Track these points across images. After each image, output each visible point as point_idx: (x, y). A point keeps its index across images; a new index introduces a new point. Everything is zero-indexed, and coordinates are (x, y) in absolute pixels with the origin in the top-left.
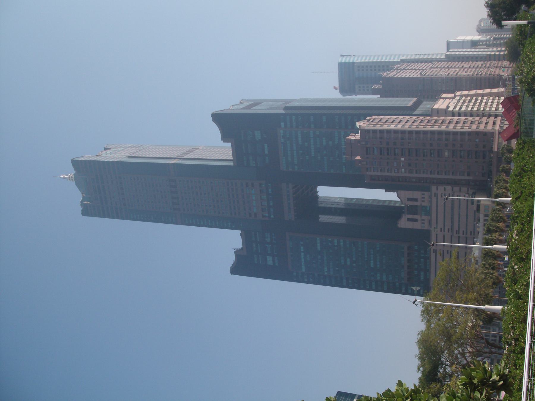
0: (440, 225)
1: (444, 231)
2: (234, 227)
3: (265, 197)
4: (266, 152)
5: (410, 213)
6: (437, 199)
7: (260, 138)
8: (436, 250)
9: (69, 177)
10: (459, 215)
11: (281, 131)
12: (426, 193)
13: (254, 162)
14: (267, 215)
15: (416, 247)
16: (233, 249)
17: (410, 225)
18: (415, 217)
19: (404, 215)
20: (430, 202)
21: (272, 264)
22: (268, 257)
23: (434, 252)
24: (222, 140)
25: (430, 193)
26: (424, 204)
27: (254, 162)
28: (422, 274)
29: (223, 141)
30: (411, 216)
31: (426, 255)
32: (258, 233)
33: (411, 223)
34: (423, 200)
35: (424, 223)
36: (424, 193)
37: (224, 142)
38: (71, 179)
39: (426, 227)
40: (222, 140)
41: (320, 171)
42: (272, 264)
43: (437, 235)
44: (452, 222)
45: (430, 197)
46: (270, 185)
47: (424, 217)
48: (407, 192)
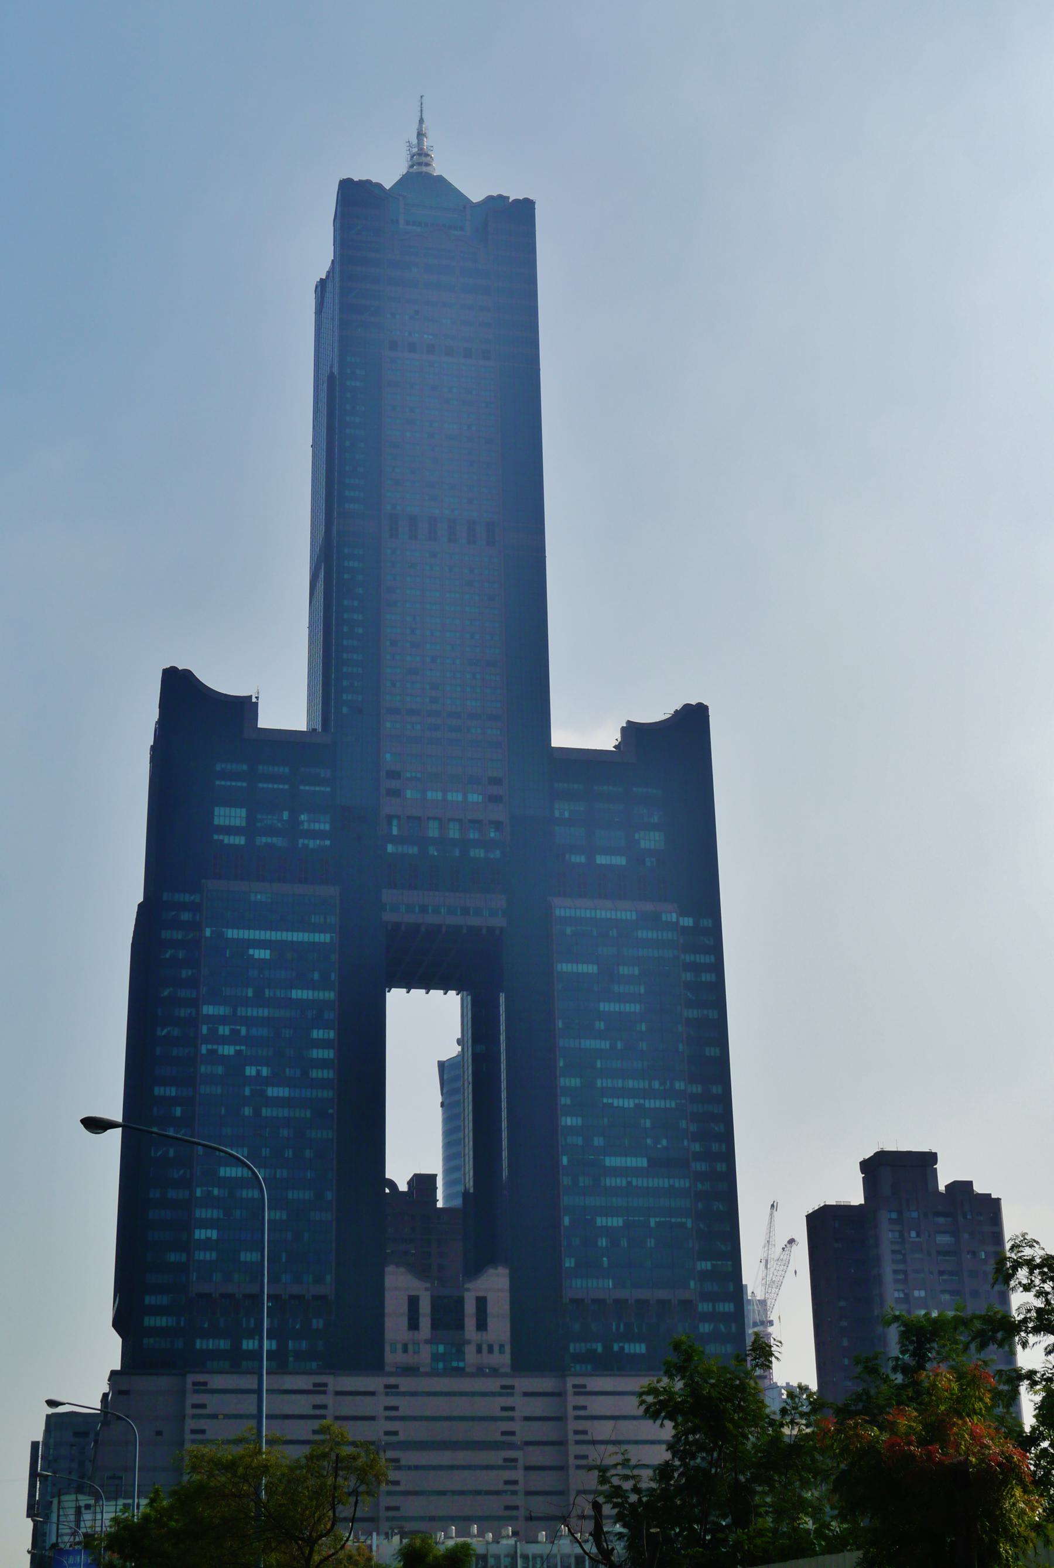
0: (406, 1406)
1: (388, 1418)
2: (345, 710)
3: (454, 832)
4: (601, 860)
5: (436, 1305)
6: (493, 1394)
8: (324, 1392)
10: (452, 1467)
11: (674, 917)
12: (506, 1358)
14: (395, 831)
15: (317, 1324)
16: (258, 693)
17: (395, 1306)
18: (425, 1323)
19: (428, 1285)
20: (480, 1372)
21: (216, 822)
22: (243, 812)
23: (315, 1385)
24: (629, 722)
25: (508, 1370)
26: (470, 1351)
27: (567, 815)
28: (223, 1344)
29: (625, 725)
30: (425, 1307)
31: (291, 1359)
32: (328, 789)
33: (404, 1308)
34: (485, 1348)
35: (405, 1350)
36: (508, 1349)
39: (392, 1357)
41: (560, 1024)
42: (216, 822)
43: (372, 1394)
44: (421, 1445)
45: (495, 1372)
46: (498, 854)
47: (426, 1351)
48: (506, 1296)
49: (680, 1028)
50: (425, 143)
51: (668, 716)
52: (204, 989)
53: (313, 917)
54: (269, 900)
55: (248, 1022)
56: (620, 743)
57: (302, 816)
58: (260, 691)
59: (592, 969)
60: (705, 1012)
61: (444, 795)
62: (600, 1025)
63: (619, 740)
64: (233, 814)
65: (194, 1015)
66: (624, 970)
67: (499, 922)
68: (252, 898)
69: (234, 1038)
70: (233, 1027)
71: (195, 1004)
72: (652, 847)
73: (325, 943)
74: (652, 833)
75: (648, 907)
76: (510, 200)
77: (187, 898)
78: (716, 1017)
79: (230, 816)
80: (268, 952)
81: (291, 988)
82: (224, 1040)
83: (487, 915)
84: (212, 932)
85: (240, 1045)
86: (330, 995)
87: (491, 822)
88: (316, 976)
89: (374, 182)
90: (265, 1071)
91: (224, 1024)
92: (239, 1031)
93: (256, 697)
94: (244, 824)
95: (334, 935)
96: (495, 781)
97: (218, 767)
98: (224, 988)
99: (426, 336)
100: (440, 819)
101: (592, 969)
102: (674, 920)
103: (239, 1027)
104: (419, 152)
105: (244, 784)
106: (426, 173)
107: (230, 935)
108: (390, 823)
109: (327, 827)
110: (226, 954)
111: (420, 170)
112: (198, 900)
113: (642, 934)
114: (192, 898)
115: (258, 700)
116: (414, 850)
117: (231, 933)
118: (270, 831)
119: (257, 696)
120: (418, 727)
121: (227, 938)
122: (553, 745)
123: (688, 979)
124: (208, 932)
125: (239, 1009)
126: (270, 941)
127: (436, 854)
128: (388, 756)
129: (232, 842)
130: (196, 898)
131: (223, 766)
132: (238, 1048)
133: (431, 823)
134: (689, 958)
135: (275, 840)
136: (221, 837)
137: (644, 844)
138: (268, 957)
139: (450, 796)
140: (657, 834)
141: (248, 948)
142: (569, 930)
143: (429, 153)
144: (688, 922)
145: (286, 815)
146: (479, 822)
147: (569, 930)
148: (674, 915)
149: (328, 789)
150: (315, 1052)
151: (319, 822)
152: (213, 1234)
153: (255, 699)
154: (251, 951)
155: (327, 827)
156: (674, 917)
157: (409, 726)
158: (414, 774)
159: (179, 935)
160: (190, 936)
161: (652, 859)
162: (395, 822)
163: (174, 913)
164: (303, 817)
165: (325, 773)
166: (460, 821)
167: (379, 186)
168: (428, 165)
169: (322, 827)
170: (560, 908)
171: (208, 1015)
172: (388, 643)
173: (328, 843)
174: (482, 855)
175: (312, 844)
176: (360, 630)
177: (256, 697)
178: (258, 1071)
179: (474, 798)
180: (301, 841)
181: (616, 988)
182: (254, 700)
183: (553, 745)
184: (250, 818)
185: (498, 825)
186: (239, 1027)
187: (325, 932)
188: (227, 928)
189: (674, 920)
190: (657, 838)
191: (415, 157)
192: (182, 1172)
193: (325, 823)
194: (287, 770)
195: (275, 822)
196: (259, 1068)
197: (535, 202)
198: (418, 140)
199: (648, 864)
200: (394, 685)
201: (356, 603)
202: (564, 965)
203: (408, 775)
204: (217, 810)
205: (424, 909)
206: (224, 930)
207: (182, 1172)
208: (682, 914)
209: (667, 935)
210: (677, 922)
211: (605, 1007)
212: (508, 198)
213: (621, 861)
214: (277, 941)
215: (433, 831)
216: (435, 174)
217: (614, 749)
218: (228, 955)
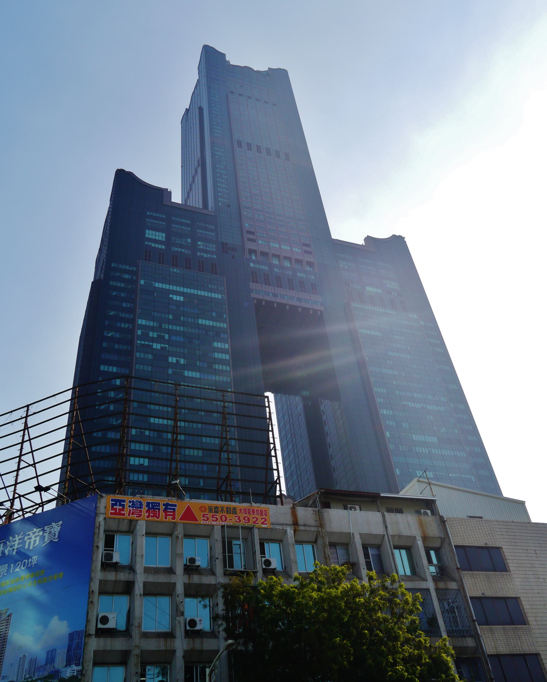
21: (147, 236)
42: (147, 236)
55: (168, 331)
65: (131, 327)
69: (160, 339)
70: (160, 334)
82: (153, 340)
85: (164, 344)
90: (182, 361)
91: (153, 331)
92: (164, 336)
124: (142, 282)
126: (183, 292)
128: (247, 225)
132: (163, 345)
135: (183, 250)
136: (150, 244)
150: (216, 354)
152: (146, 462)
154: (171, 296)
160: (129, 287)
163: (119, 274)
173: (215, 256)
178: (177, 361)
184: (167, 237)
188: (155, 282)
192: (119, 422)
195: (183, 242)
196: (178, 359)
203: (259, 235)
206: (152, 282)
207: (119, 422)
218: (155, 296)
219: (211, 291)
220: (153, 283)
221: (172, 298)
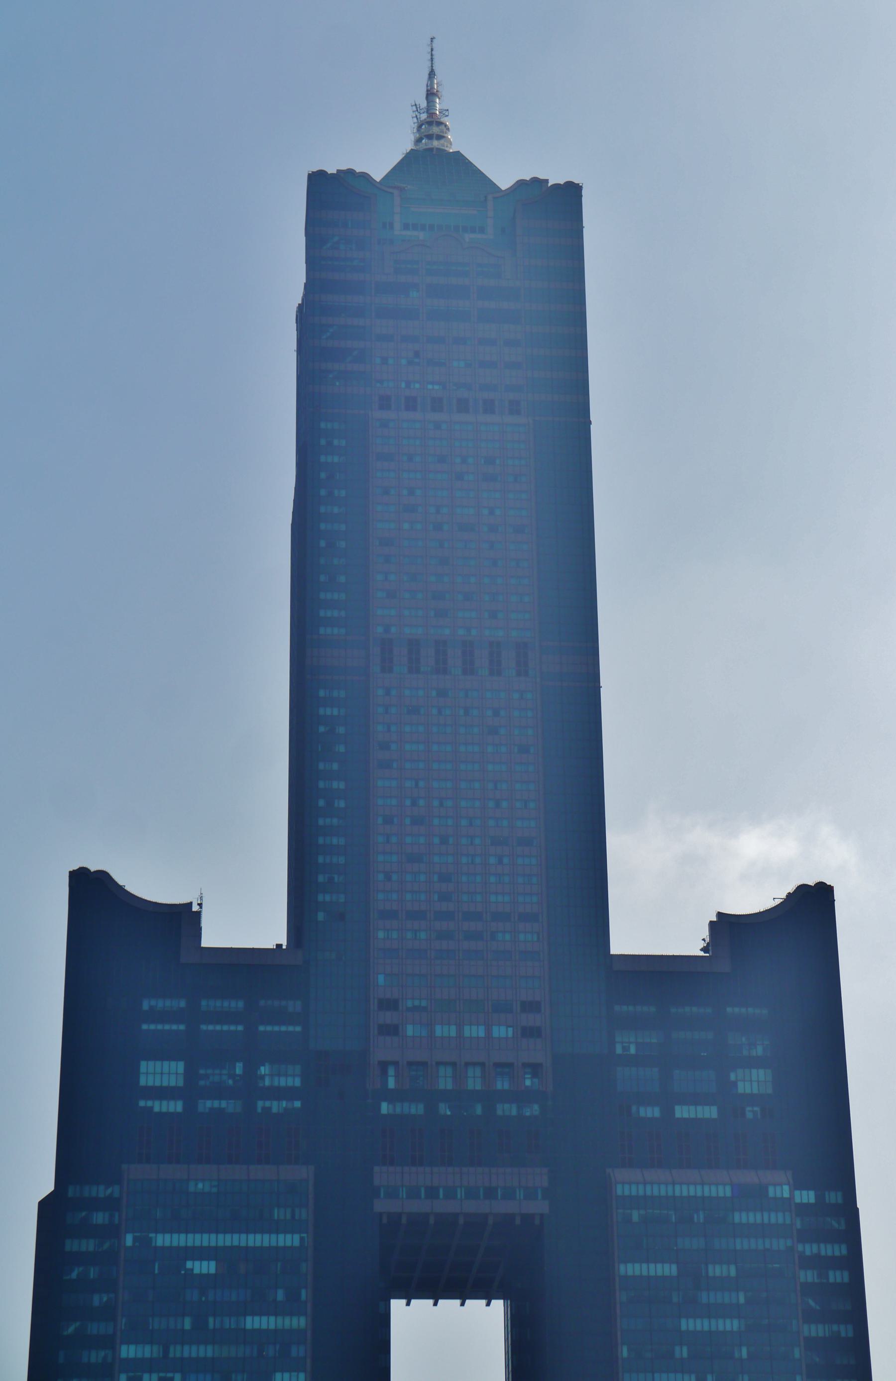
3: (474, 1082)
4: (682, 1112)
7: (742, 1088)
9: (440, 123)
11: (786, 1192)
13: (633, 1050)
14: (391, 1083)
16: (201, 899)
21: (143, 1082)
22: (180, 1066)
24: (720, 915)
27: (633, 1050)
29: (715, 919)
32: (298, 1029)
37: (711, 923)
38: (435, 130)
40: (720, 915)
41: (625, 1352)
42: (143, 1082)
49: (797, 1354)
50: (438, 106)
51: (778, 902)
52: (124, 1321)
53: (276, 1211)
54: (214, 1190)
56: (708, 944)
57: (262, 1068)
58: (203, 895)
59: (669, 1270)
60: (835, 1328)
61: (460, 1030)
62: (683, 1352)
63: (708, 940)
64: (166, 1070)
66: (716, 1270)
67: (539, 1207)
68: (192, 1188)
71: (109, 1343)
72: (755, 1091)
73: (292, 1248)
74: (754, 1071)
75: (748, 1177)
76: (549, 185)
77: (101, 1191)
78: (851, 1334)
79: (162, 1074)
80: (213, 1264)
81: (245, 1315)
83: (522, 1197)
84: (135, 1239)
86: (299, 1322)
87: (525, 1065)
88: (280, 1295)
89: (357, 171)
93: (198, 904)
94: (181, 1083)
95: (305, 1235)
96: (530, 1007)
97: (146, 1006)
98: (150, 1319)
99: (430, 387)
100: (454, 1065)
101: (669, 1270)
102: (786, 1194)
103: (170, 1375)
104: (429, 120)
105: (182, 1027)
106: (438, 149)
107: (159, 1243)
108: (384, 1073)
109: (298, 1082)
110: (154, 1270)
111: (430, 146)
112: (116, 1195)
113: (741, 1218)
114: (109, 1191)
115: (201, 907)
116: (417, 1109)
117: (162, 1240)
118: (219, 1092)
119: (199, 902)
120: (423, 935)
121: (156, 1247)
122: (612, 953)
123: (810, 1280)
124: (129, 1240)
125: (172, 1349)
126: (216, 1248)
127: (449, 1113)
128: (381, 979)
129: (164, 1110)
130: (114, 1191)
131: (153, 1003)
133: (442, 1070)
134: (810, 1249)
135: (224, 1104)
136: (149, 1103)
137: (743, 1088)
138: (213, 1270)
139: (467, 1031)
140: (761, 1072)
141: (186, 1260)
142: (635, 1216)
143: (443, 120)
144: (807, 1197)
145: (239, 1069)
146: (510, 1065)
147: (635, 1216)
148: (786, 1188)
149: (298, 1029)
151: (286, 1076)
153: (198, 907)
154: (189, 1264)
155: (298, 1082)
156: (786, 1192)
157: (409, 935)
158: (417, 1003)
159: (88, 1245)
160: (106, 1246)
161: (756, 1109)
162: (391, 1071)
164: (263, 1070)
165: (294, 1006)
166: (483, 1065)
167: (365, 176)
168: (440, 137)
169: (290, 1082)
170: (623, 1183)
171: (127, 1360)
172: (380, 820)
173: (298, 1104)
174: (514, 1112)
175: (276, 1106)
176: (342, 804)
177: (198, 904)
179: (501, 1032)
180: (260, 1104)
181: (704, 1297)
182: (195, 908)
183: (612, 953)
184: (190, 1075)
185: (535, 1069)
186: (170, 1375)
187: (293, 1232)
188: (156, 1232)
189: (786, 1194)
190: (762, 1078)
191: (423, 127)
193: (294, 1076)
194: (241, 1004)
195: (225, 1078)
197: (581, 187)
198: (428, 103)
199: (749, 1115)
200: (388, 878)
201: (335, 766)
202: (630, 1266)
203: (409, 1004)
204: (143, 1064)
205: (432, 1192)
206: (152, 1235)
208: (798, 1185)
209: (777, 1218)
210: (792, 1197)
211: (687, 1325)
212: (547, 181)
213: (710, 1112)
214: (225, 1248)
215: (445, 1081)
216: (451, 151)
217: (702, 954)
218: (156, 1272)
219: (276, 1228)
220: (151, 1238)
221: (192, 1270)
